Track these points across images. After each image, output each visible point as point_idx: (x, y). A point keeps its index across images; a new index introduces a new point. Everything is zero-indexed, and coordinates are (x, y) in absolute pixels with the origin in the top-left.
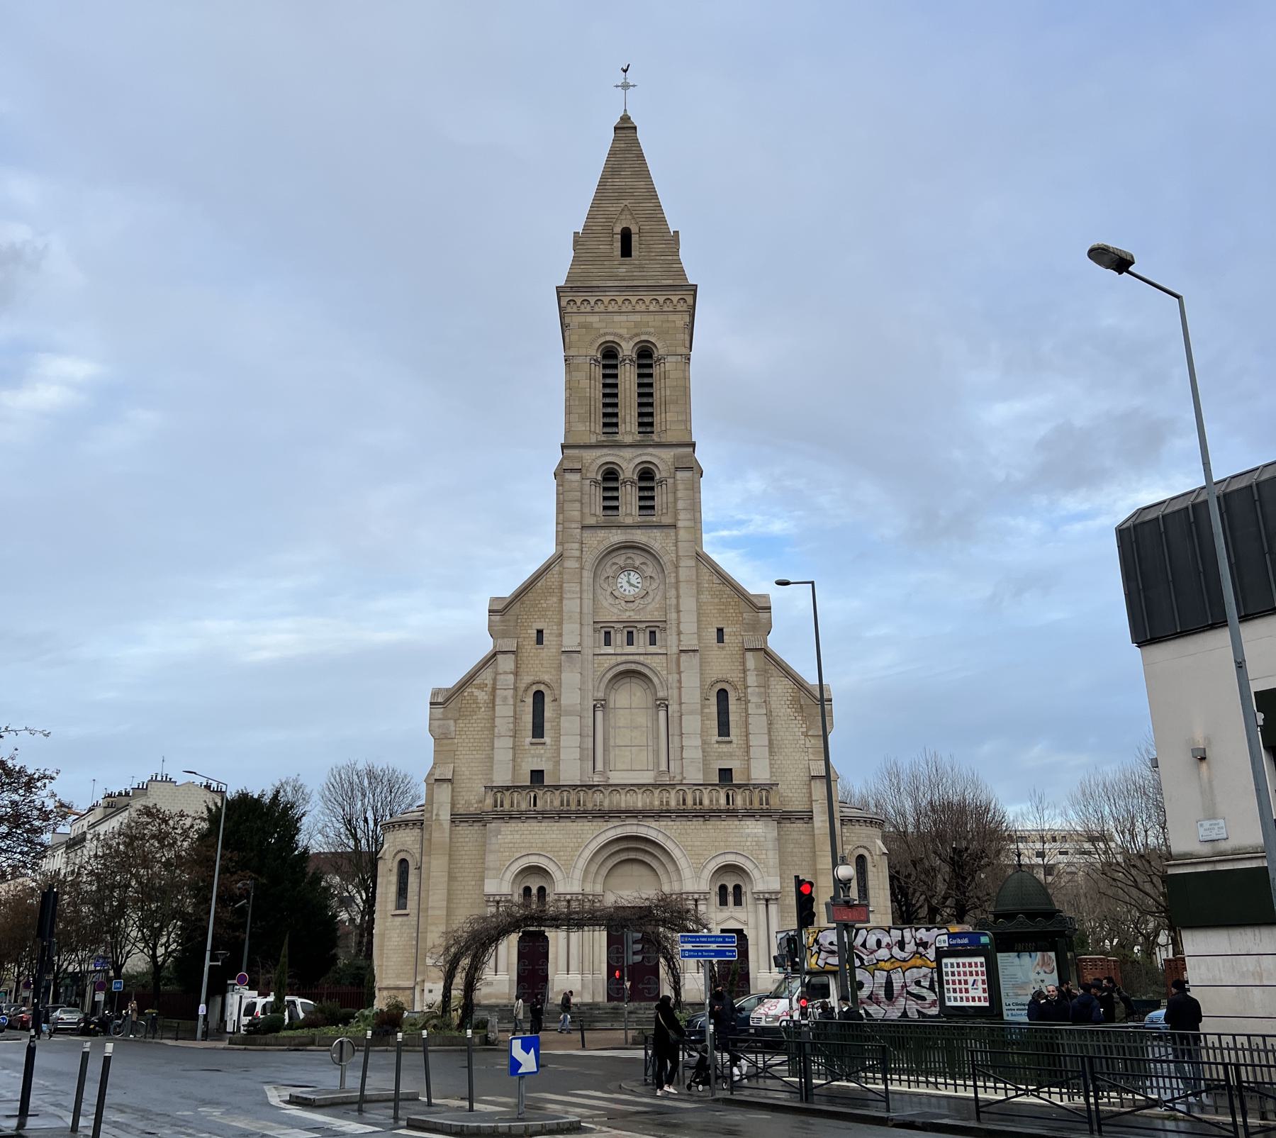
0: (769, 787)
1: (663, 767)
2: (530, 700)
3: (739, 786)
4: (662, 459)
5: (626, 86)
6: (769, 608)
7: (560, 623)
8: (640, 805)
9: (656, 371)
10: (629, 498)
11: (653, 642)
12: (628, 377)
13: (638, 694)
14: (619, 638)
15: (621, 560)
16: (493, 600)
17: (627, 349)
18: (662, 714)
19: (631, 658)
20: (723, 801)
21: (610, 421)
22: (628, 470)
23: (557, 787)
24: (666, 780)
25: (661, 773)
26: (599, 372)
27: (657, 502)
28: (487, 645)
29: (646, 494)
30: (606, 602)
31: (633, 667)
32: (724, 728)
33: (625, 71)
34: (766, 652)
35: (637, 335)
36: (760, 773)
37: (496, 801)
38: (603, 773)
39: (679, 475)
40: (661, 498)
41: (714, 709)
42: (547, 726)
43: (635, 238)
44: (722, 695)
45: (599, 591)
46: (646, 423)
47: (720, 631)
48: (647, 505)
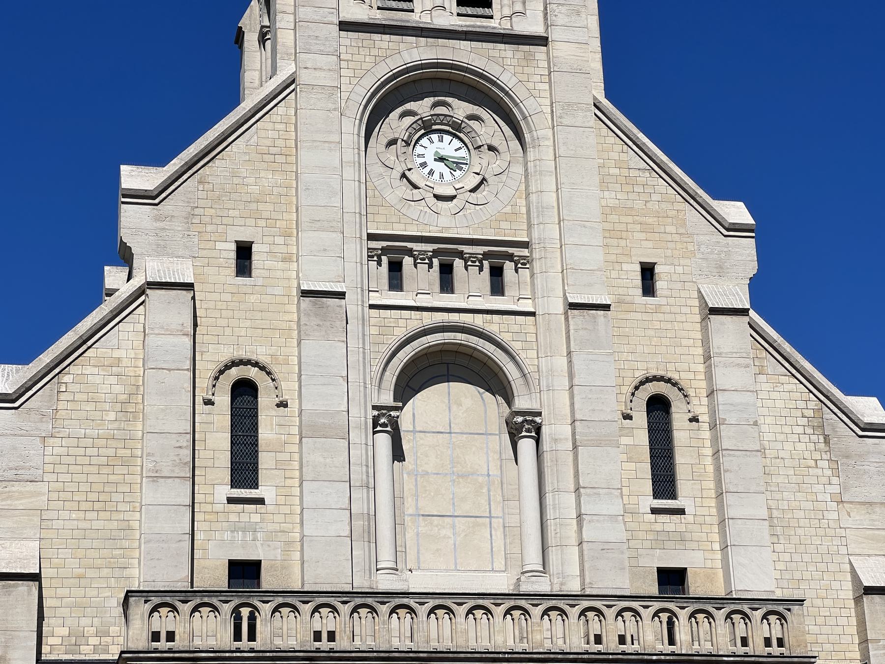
0: (779, 608)
1: (533, 560)
2: (223, 400)
11: (497, 288)
13: (467, 402)
14: (421, 280)
15: (423, 107)
18: (526, 446)
19: (454, 317)
32: (664, 482)
36: (755, 578)
41: (643, 438)
42: (265, 460)
44: (659, 406)
45: (376, 169)
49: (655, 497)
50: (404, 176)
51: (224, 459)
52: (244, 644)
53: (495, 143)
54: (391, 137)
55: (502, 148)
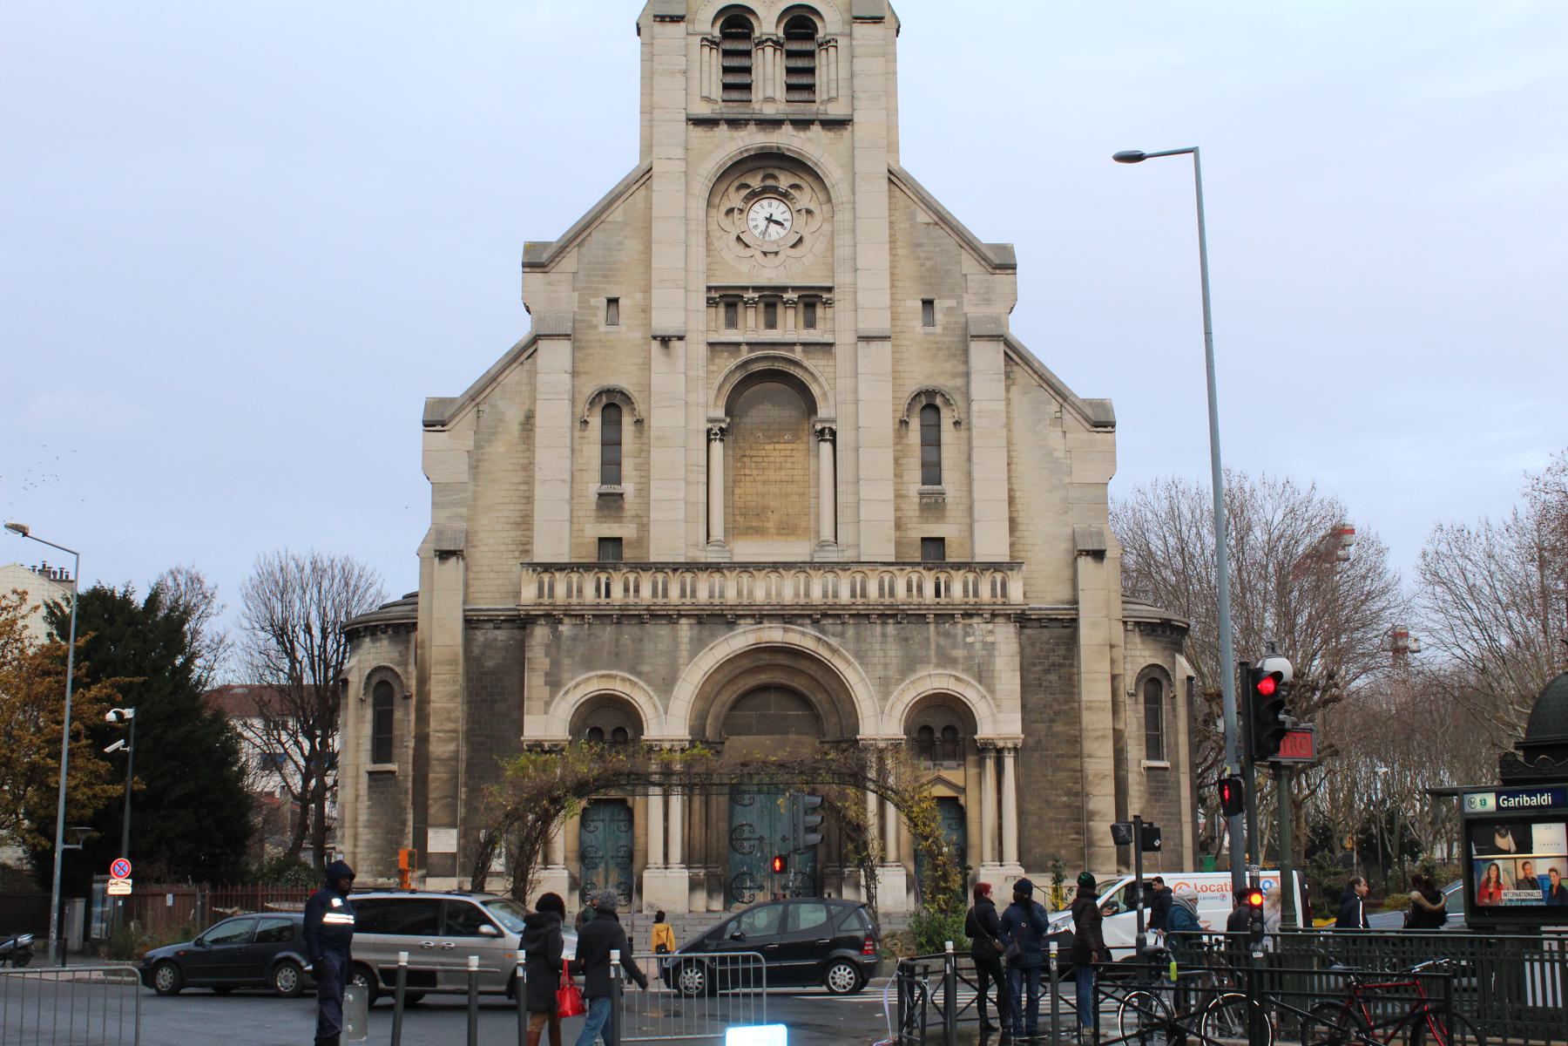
1: (827, 533)
3: (958, 566)
6: (1014, 267)
7: (647, 289)
8: (788, 596)
10: (769, 70)
11: (810, 324)
15: (756, 182)
16: (530, 248)
18: (826, 447)
20: (929, 590)
23: (645, 567)
25: (822, 545)
27: (821, 79)
28: (522, 328)
29: (800, 63)
30: (729, 250)
31: (778, 366)
34: (1008, 343)
36: (991, 544)
37: (541, 588)
38: (723, 544)
39: (860, 30)
40: (827, 69)
47: (928, 304)
48: (801, 81)
49: (924, 483)
50: (739, 238)
51: (596, 463)
52: (603, 600)
53: (811, 207)
54: (729, 206)
55: (816, 211)
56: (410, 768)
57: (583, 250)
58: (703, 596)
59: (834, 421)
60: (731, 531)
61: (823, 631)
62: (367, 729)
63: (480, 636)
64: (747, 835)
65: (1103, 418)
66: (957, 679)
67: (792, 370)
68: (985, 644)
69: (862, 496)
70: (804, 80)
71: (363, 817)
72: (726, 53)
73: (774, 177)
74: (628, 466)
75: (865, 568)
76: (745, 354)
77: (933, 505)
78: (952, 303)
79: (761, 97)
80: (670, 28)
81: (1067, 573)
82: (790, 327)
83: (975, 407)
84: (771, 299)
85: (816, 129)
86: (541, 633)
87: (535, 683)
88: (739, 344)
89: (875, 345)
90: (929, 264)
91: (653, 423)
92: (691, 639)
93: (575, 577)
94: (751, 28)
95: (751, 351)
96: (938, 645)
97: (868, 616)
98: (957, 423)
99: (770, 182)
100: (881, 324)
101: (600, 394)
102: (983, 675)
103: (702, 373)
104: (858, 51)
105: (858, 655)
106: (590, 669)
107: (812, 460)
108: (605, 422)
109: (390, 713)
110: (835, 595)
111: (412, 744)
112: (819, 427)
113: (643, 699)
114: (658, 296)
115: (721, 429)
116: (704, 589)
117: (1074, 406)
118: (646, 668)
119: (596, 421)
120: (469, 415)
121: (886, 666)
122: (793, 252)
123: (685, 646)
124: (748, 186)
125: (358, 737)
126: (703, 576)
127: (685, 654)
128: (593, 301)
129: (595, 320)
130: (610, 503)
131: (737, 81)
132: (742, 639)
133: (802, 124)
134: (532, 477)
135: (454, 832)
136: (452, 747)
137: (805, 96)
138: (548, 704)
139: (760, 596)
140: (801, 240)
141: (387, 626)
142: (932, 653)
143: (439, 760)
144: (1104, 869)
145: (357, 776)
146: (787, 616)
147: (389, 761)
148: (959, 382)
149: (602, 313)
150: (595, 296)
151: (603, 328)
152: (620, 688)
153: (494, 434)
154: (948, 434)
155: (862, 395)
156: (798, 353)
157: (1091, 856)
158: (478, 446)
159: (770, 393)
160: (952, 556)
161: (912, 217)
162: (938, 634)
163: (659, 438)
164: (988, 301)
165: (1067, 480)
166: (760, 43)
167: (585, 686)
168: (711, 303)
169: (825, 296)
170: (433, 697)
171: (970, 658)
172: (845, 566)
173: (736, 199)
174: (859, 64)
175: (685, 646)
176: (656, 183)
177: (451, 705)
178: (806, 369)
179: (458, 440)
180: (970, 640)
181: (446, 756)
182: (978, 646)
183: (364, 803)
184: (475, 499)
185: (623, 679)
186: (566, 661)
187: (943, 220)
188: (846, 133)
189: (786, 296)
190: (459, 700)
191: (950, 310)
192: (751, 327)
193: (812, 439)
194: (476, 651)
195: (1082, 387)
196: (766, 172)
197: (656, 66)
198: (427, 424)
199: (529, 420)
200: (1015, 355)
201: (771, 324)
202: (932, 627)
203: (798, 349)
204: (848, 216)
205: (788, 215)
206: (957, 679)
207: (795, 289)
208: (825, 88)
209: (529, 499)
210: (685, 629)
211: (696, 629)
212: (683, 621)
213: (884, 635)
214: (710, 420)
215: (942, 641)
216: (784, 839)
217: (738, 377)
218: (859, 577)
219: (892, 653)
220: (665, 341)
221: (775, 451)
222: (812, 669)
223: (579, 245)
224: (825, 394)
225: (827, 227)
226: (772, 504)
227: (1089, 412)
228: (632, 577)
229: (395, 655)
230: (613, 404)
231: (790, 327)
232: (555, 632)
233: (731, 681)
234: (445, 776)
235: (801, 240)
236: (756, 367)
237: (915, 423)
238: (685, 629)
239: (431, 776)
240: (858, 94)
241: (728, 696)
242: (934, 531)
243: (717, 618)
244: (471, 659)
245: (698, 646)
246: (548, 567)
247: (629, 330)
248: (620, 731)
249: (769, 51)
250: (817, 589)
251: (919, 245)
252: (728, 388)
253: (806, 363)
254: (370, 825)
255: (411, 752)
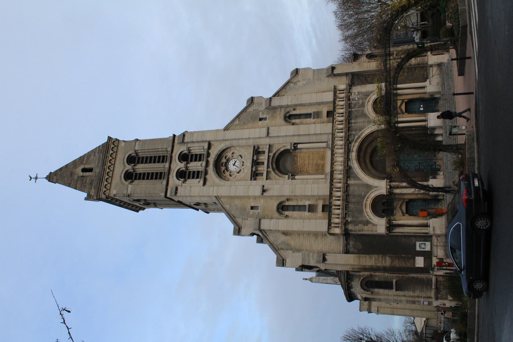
1: (324, 145)
4: (179, 149)
5: (36, 178)
7: (249, 197)
9: (141, 155)
10: (195, 166)
11: (264, 152)
12: (141, 168)
15: (223, 168)
16: (235, 234)
17: (129, 167)
18: (299, 146)
21: (158, 176)
22: (181, 166)
24: (330, 143)
25: (328, 145)
26: (136, 182)
29: (194, 158)
31: (274, 160)
33: (31, 177)
35: (124, 163)
36: (329, 97)
39: (186, 140)
40: (196, 150)
43: (87, 166)
46: (161, 159)
47: (261, 119)
48: (198, 158)
49: (311, 118)
50: (238, 173)
53: (231, 153)
54: (229, 176)
56: (395, 275)
57: (236, 216)
58: (341, 176)
59: (291, 143)
60: (323, 172)
61: (353, 140)
62: (381, 291)
63: (351, 250)
64: (418, 167)
65: (295, 72)
66: (368, 101)
67: (276, 156)
68: (358, 95)
69: (313, 133)
70: (198, 157)
71: (411, 293)
72: (189, 178)
73: (223, 163)
74: (300, 203)
75: (334, 129)
76: (270, 169)
77: (317, 115)
78: (261, 113)
79: (200, 168)
80: (179, 191)
81: (338, 78)
82: (264, 158)
83: (289, 104)
84: (256, 163)
85: (210, 151)
86: (350, 227)
87: (367, 230)
88: (267, 171)
89: (270, 131)
90: (250, 120)
91: (288, 194)
92: (354, 180)
93: (333, 216)
94: (183, 171)
95: (269, 168)
96: (358, 108)
97: (349, 128)
98: (294, 110)
99: (224, 165)
100: (264, 130)
101: (279, 212)
102: (367, 95)
103: (274, 181)
104: (191, 140)
105: (361, 130)
106: (363, 212)
107: (303, 150)
108: (287, 210)
109: (376, 282)
110: (342, 137)
111: (387, 274)
112: (293, 148)
113: (373, 195)
114: (251, 193)
115: (292, 176)
116: (339, 176)
117: (291, 79)
118: (363, 194)
119: (286, 213)
120: (282, 252)
121: (364, 122)
122: (243, 158)
123: (356, 182)
124: (224, 171)
125: (384, 295)
126: (335, 176)
127: (359, 182)
128: (251, 214)
129: (257, 213)
130: (312, 209)
131: (196, 175)
132: (355, 165)
133: (208, 155)
134: (302, 231)
135: (417, 258)
136: (388, 258)
137: (202, 156)
138: (374, 225)
139: (341, 159)
140: (240, 156)
141: (347, 282)
142: (360, 109)
143: (392, 263)
144: (427, 60)
145: (397, 295)
146: (348, 151)
147: (392, 282)
148: (283, 110)
149: (255, 211)
150: (249, 213)
151: (259, 211)
152: (369, 202)
153: (288, 244)
154: (297, 112)
155: (283, 135)
156: (271, 154)
157: (423, 64)
158: (291, 249)
159: (283, 162)
160: (331, 109)
161: (236, 125)
162: (355, 108)
163: (292, 192)
164: (261, 104)
165: (312, 80)
166: (187, 168)
167: (368, 213)
168: (255, 179)
169: (256, 148)
170: (370, 264)
171: (362, 99)
172: (333, 134)
173: (227, 174)
174: (194, 140)
175: (356, 182)
176: (220, 194)
177: (373, 258)
178: (276, 152)
179: (289, 256)
180: (357, 99)
181: (390, 260)
182: (359, 96)
183: (406, 293)
184: (308, 251)
185: (366, 201)
186: (360, 219)
187: (238, 116)
188: (212, 143)
189: (255, 159)
190: (372, 256)
191: (263, 113)
192: (263, 169)
193: (297, 151)
194: (356, 251)
195: (288, 77)
196: (220, 165)
197: (188, 195)
198: (283, 265)
199: (285, 233)
200: (277, 94)
201: (263, 163)
202: (353, 110)
203: (270, 154)
204: (234, 141)
205: (233, 160)
206: (368, 101)
207: (253, 156)
208: (201, 151)
209: (309, 233)
210: (351, 182)
211: (351, 178)
212: (348, 182)
213: (355, 123)
214: (289, 179)
215: (357, 107)
216: (419, 156)
217: (277, 172)
218: (337, 131)
219: (360, 121)
220: (264, 191)
221: (300, 161)
222: (365, 145)
223: (235, 217)
224: (284, 147)
225: (237, 148)
226: (315, 162)
227: (293, 75)
228: (334, 198)
229: (357, 279)
230: (282, 208)
231: (264, 158)
232: (350, 223)
233: (369, 170)
234: (397, 261)
235: (240, 156)
236: (274, 166)
237: (293, 121)
238: (351, 182)
239: (397, 265)
240: (202, 140)
241: (373, 171)
242: (325, 114)
243: (348, 172)
244: (359, 252)
245: (356, 178)
246: (330, 224)
247: (260, 203)
248: (383, 204)
249: (189, 165)
250: (340, 143)
251: (244, 123)
252: (280, 174)
253: (274, 152)
254: (414, 291)
255: (389, 275)
